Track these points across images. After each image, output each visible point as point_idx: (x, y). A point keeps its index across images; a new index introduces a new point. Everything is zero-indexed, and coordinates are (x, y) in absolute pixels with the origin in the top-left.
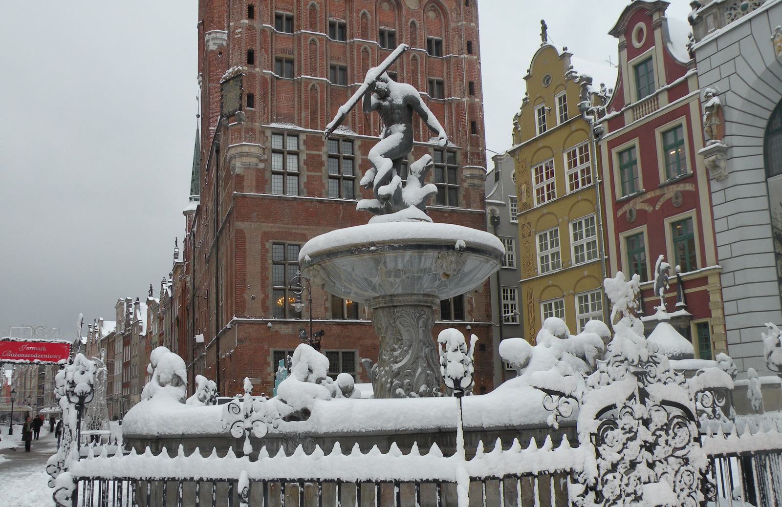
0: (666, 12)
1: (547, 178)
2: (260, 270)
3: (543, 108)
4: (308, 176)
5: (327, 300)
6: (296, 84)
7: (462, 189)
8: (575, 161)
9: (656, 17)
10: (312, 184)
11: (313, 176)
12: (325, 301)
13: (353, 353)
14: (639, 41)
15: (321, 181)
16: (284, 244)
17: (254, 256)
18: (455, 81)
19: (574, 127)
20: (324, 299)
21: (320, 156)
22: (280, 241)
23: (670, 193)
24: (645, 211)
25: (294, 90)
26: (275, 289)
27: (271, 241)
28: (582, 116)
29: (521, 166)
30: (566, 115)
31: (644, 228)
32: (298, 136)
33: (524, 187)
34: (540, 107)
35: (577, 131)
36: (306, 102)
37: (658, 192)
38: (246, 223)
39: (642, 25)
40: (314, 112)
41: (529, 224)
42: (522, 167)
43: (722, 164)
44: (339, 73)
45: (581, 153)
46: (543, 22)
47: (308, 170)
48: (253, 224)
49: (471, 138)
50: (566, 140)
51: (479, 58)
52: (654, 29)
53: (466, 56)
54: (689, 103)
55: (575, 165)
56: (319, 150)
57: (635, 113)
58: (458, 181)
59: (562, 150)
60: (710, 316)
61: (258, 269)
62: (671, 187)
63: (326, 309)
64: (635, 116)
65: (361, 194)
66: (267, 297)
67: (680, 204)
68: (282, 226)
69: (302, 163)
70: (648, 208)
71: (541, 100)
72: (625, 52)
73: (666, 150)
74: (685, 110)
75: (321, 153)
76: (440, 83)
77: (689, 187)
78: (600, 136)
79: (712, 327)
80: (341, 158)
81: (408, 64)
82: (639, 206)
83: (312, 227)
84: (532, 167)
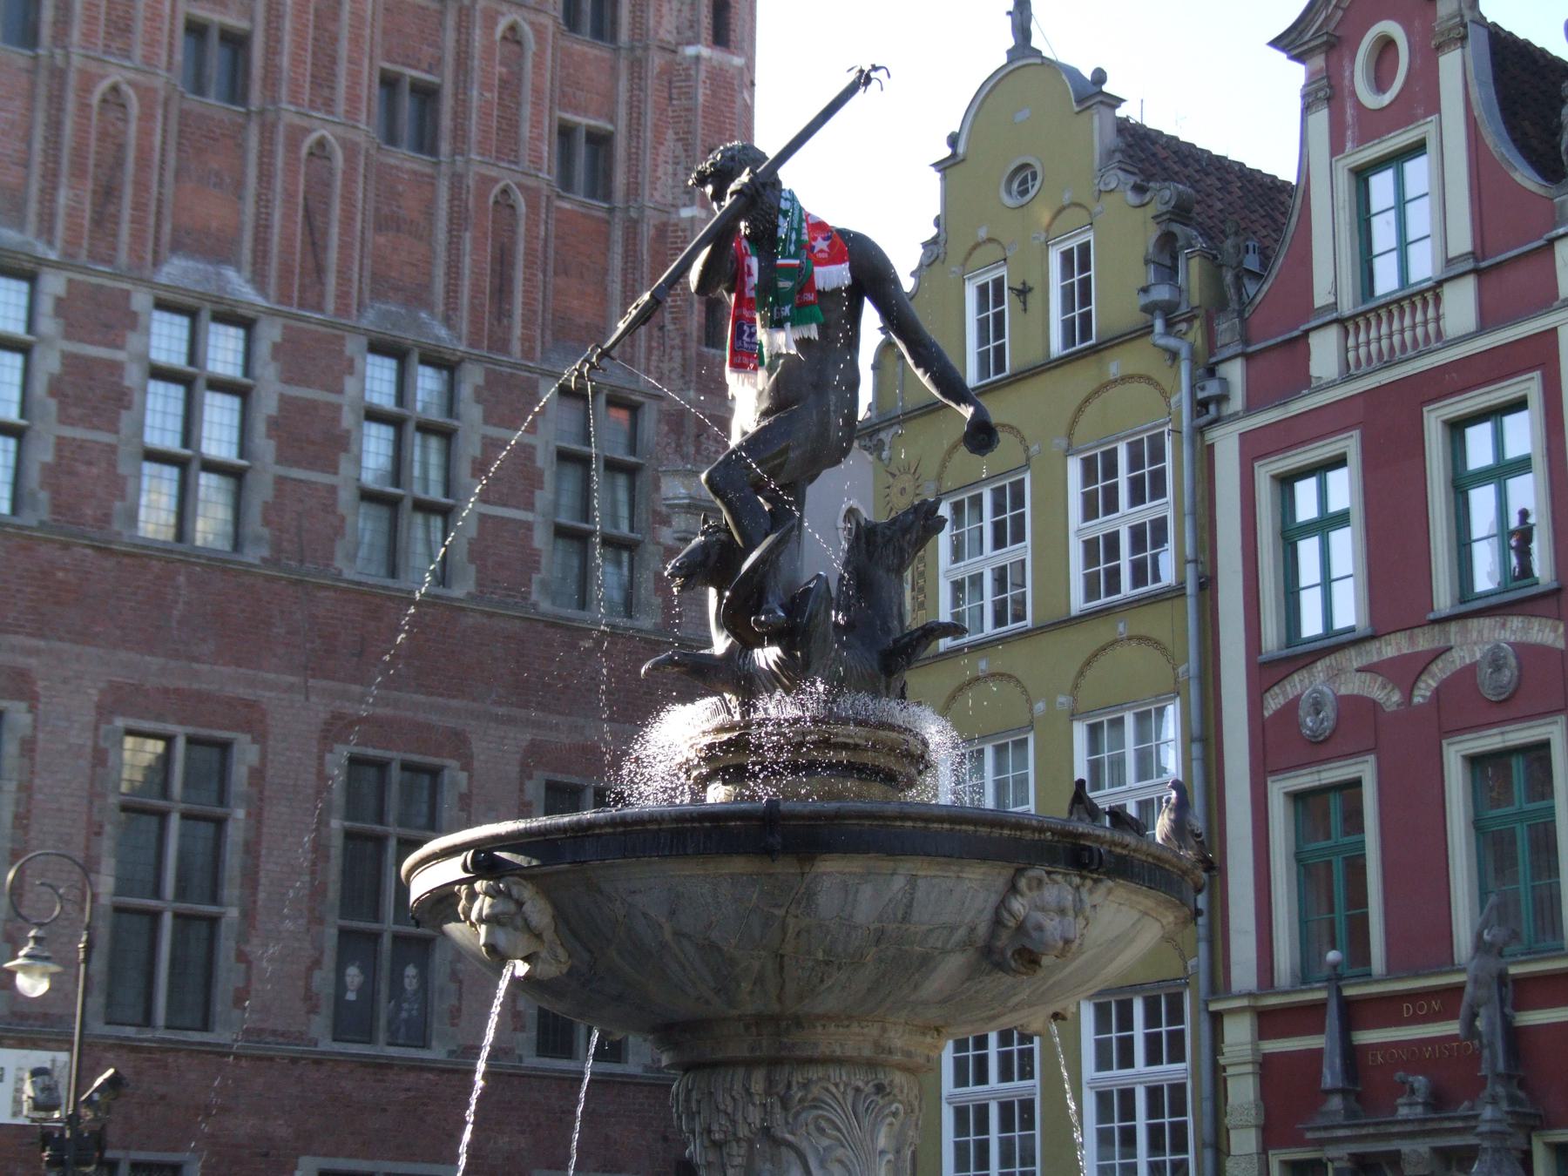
1: (999, 543)
3: (999, 283)
4: (61, 442)
6: (43, 79)
7: (651, 548)
8: (1111, 493)
11: (81, 445)
14: (1380, 85)
15: (112, 465)
18: (659, 141)
19: (1115, 365)
21: (115, 367)
24: (1375, 705)
25: (31, 97)
28: (1148, 329)
29: (895, 490)
30: (1086, 318)
31: (1365, 770)
32: (31, 278)
34: (989, 277)
35: (1125, 379)
36: (79, 152)
37: (1424, 641)
40: (107, 193)
44: (216, 55)
45: (1136, 462)
47: (65, 419)
49: (700, 355)
50: (1080, 410)
51: (750, 66)
52: (1440, 48)
53: (705, 52)
54: (1555, 329)
55: (1111, 506)
56: (118, 345)
57: (1351, 342)
58: (643, 514)
59: (1064, 443)
62: (1474, 624)
64: (1351, 355)
65: (265, 532)
67: (1511, 689)
69: (40, 387)
70: (1389, 698)
71: (992, 251)
72: (1321, 118)
75: (120, 356)
76: (600, 141)
78: (1212, 408)
80: (201, 384)
81: (488, 51)
82: (1354, 685)
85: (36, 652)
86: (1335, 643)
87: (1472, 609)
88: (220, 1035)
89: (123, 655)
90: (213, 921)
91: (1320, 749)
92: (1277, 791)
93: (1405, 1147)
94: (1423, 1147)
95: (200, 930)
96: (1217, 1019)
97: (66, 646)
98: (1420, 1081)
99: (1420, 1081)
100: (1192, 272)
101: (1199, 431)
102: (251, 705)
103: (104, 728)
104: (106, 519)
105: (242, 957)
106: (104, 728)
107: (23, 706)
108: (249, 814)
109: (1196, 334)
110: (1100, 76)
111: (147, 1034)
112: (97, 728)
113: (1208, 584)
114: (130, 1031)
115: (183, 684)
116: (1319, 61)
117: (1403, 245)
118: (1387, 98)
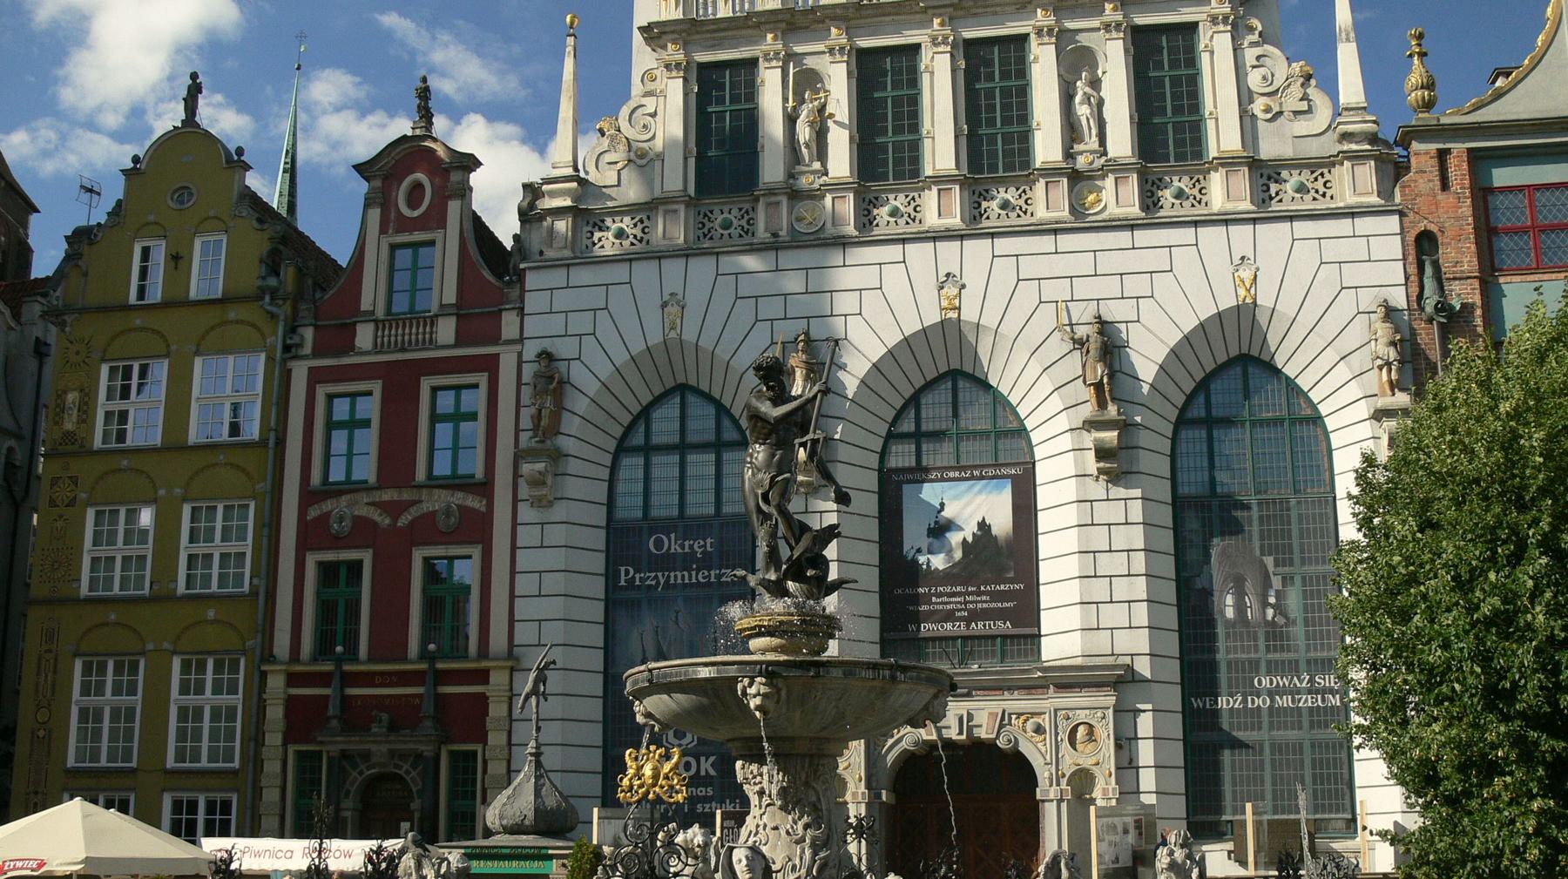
0: (473, 176)
9: (455, 177)
14: (413, 202)
23: (437, 501)
24: (375, 523)
33: (72, 397)
35: (237, 322)
37: (407, 495)
39: (420, 176)
41: (74, 480)
42: (77, 353)
43: (549, 480)
46: (194, 76)
52: (450, 197)
60: (485, 743)
62: (436, 491)
72: (375, 214)
73: (435, 418)
74: (490, 365)
77: (474, 502)
79: (485, 762)
82: (363, 511)
84: (104, 360)
86: (352, 487)
87: (434, 482)
91: (338, 542)
92: (311, 560)
93: (374, 748)
94: (384, 748)
96: (264, 675)
98: (385, 716)
99: (385, 716)
100: (289, 273)
101: (284, 361)
109: (288, 307)
110: (240, 151)
113: (281, 443)
116: (378, 183)
117: (414, 290)
118: (416, 214)
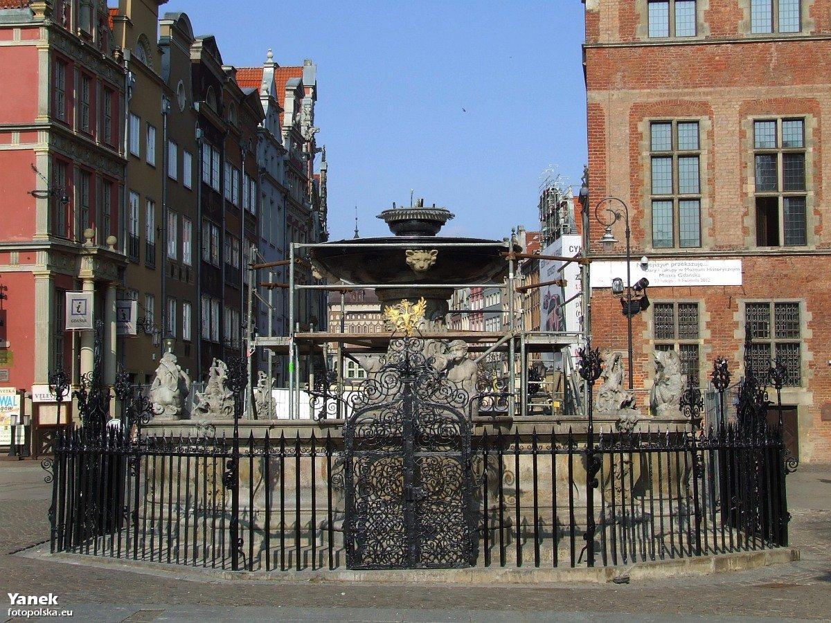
2: (629, 170)
5: (746, 214)
10: (719, 12)
12: (742, 217)
13: (796, 305)
16: (670, 122)
17: (619, 147)
20: (741, 213)
22: (663, 118)
26: (654, 200)
27: (647, 119)
38: (604, 92)
48: (615, 92)
61: (626, 168)
63: (745, 231)
65: (812, 20)
66: (641, 213)
68: (666, 91)
83: (718, 89)
85: (711, 93)
88: (811, 247)
89: (749, 88)
90: (803, 198)
95: (798, 203)
97: (722, 88)
102: (811, 100)
103: (743, 121)
104: (736, 29)
105: (817, 212)
106: (743, 121)
107: (707, 117)
108: (814, 149)
111: (775, 249)
112: (740, 122)
114: (768, 249)
115: (778, 96)
